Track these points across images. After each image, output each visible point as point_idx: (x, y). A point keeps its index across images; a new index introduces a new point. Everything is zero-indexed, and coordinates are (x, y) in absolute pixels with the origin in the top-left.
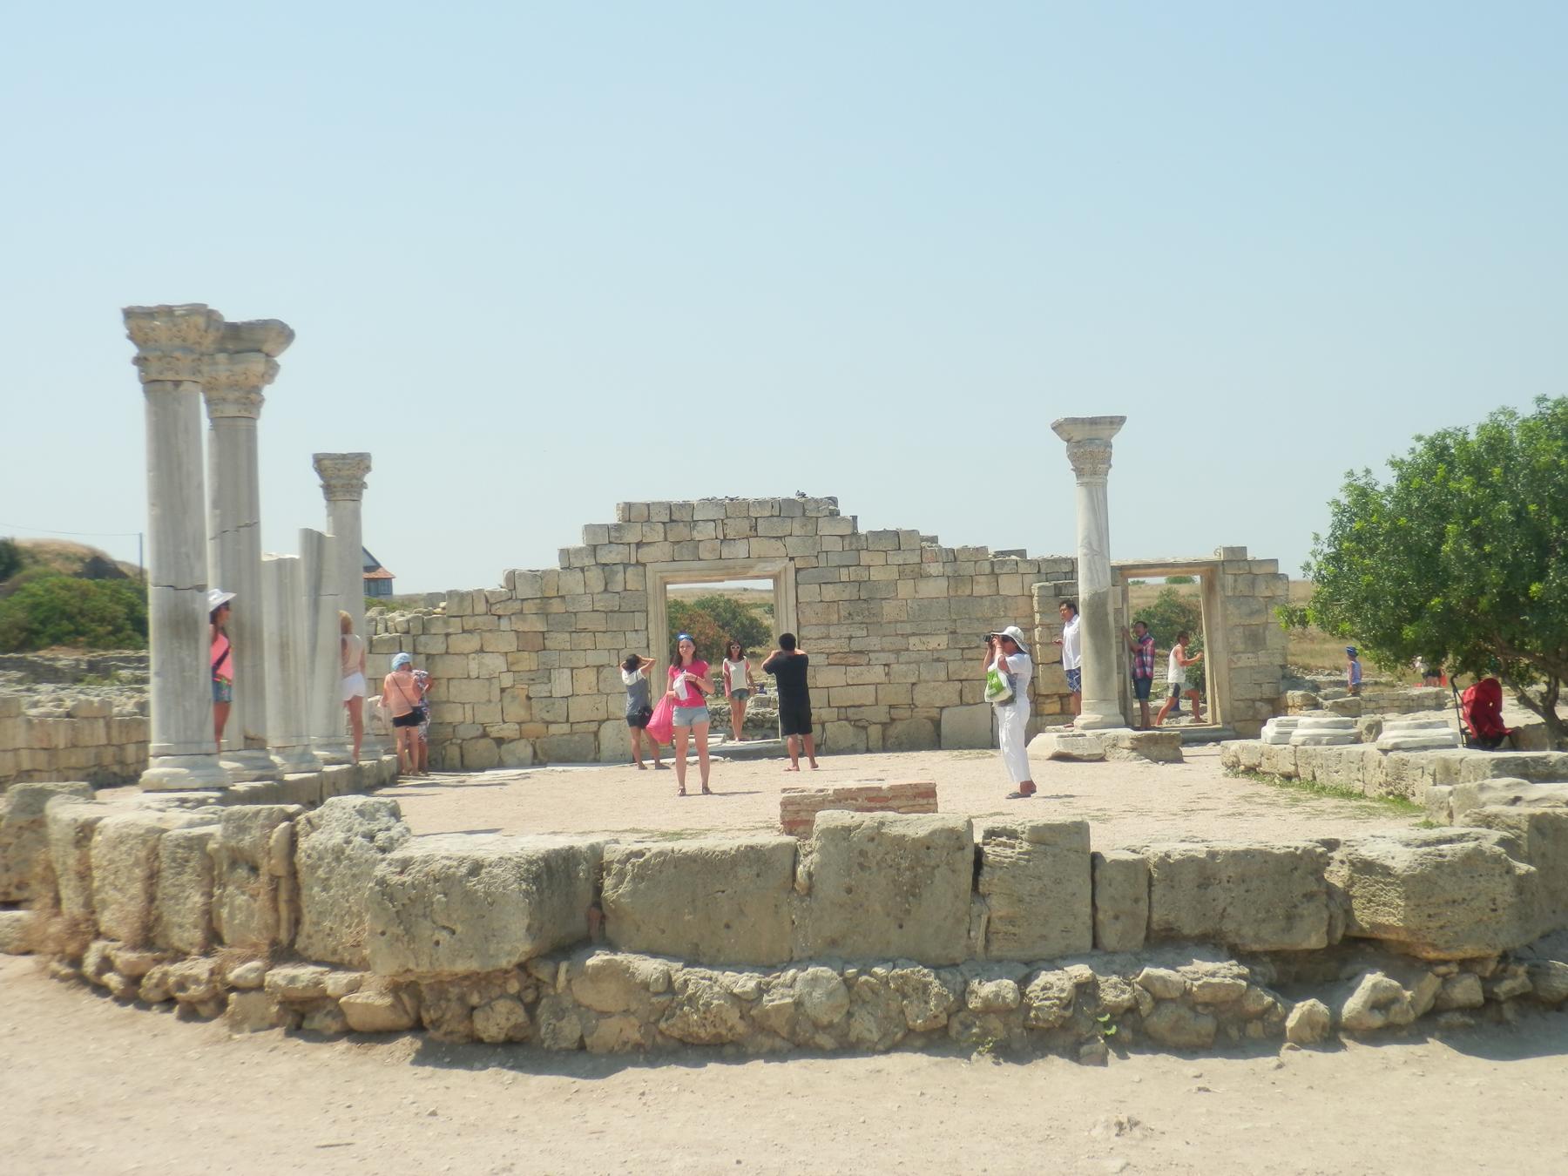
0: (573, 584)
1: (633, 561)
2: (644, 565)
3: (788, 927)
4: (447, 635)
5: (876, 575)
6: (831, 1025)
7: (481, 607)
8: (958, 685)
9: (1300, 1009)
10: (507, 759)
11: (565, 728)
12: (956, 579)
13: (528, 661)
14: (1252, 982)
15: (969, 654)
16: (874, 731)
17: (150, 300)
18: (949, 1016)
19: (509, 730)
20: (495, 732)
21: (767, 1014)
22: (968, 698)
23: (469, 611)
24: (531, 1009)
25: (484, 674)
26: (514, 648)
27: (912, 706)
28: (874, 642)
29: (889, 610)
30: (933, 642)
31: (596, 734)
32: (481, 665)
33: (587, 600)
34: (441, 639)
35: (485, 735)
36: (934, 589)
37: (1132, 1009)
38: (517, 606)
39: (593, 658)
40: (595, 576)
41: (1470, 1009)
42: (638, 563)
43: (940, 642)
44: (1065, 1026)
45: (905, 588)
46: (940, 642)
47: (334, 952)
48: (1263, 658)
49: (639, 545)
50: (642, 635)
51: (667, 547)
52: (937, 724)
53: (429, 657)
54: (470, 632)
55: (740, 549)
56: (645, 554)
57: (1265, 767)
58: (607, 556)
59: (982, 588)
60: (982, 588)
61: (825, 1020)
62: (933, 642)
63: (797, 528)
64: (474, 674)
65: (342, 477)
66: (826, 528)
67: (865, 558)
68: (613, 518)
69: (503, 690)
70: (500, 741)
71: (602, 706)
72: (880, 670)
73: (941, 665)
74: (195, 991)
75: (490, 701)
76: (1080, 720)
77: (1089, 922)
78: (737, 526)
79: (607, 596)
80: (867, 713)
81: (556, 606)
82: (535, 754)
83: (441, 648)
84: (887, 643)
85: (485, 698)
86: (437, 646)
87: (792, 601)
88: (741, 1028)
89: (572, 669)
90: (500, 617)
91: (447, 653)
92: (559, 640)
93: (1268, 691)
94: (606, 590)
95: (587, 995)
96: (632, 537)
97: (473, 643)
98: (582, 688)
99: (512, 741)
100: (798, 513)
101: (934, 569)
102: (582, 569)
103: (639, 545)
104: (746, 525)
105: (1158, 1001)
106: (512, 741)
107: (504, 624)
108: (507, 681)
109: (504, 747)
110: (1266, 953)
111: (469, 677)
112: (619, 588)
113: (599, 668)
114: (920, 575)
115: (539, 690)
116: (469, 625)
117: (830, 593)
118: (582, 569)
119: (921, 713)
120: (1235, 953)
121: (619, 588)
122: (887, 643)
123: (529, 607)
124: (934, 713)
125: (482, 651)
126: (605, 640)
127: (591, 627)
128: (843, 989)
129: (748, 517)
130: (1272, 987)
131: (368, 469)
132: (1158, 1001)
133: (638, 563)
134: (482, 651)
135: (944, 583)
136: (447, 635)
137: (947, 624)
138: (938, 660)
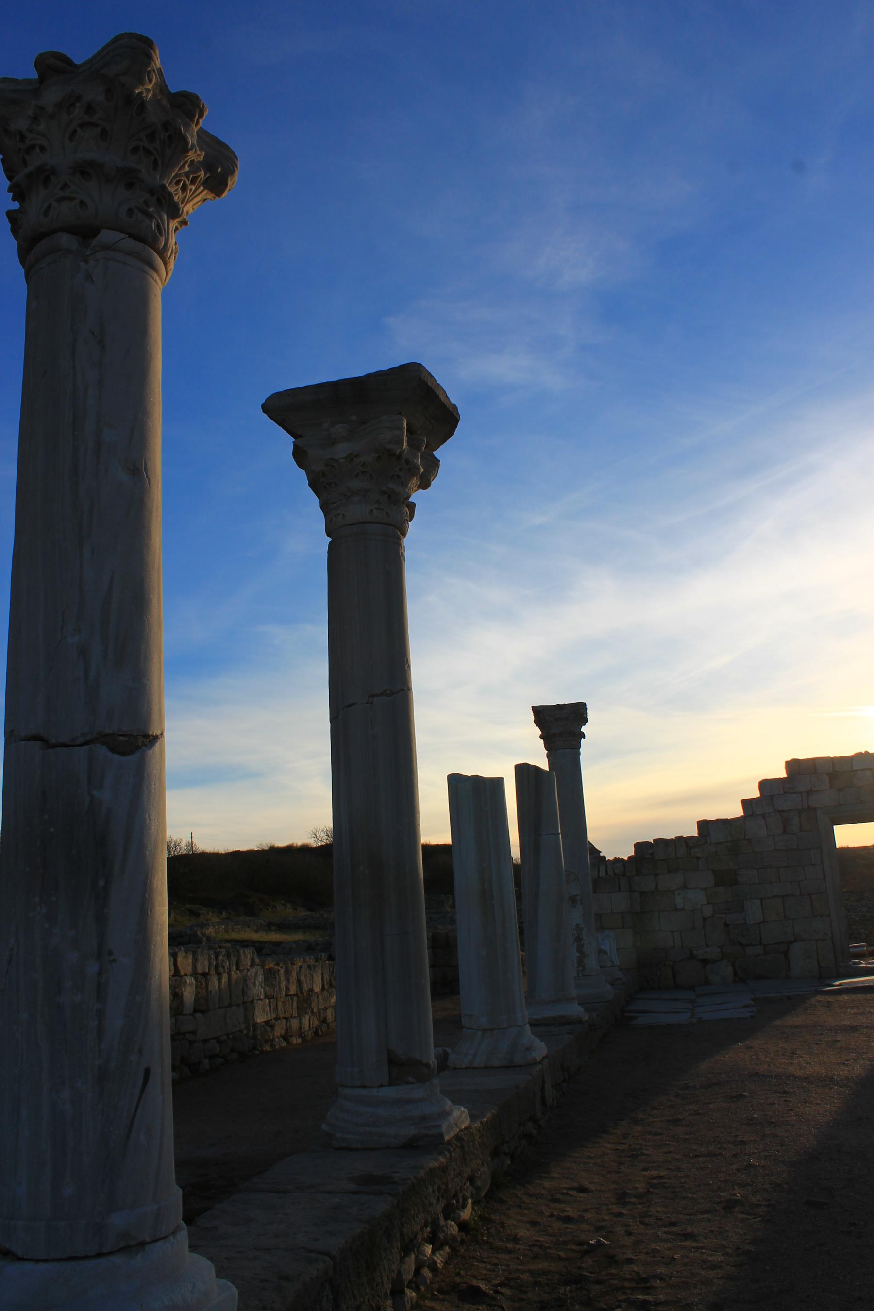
2: (815, 809)
4: (656, 875)
35: (692, 957)
53: (642, 894)
68: (781, 773)
69: (705, 919)
70: (705, 962)
82: (735, 973)
89: (762, 899)
94: (785, 832)
102: (764, 816)
108: (708, 911)
111: (676, 909)
118: (764, 816)
125: (685, 887)
131: (585, 721)
134: (685, 887)
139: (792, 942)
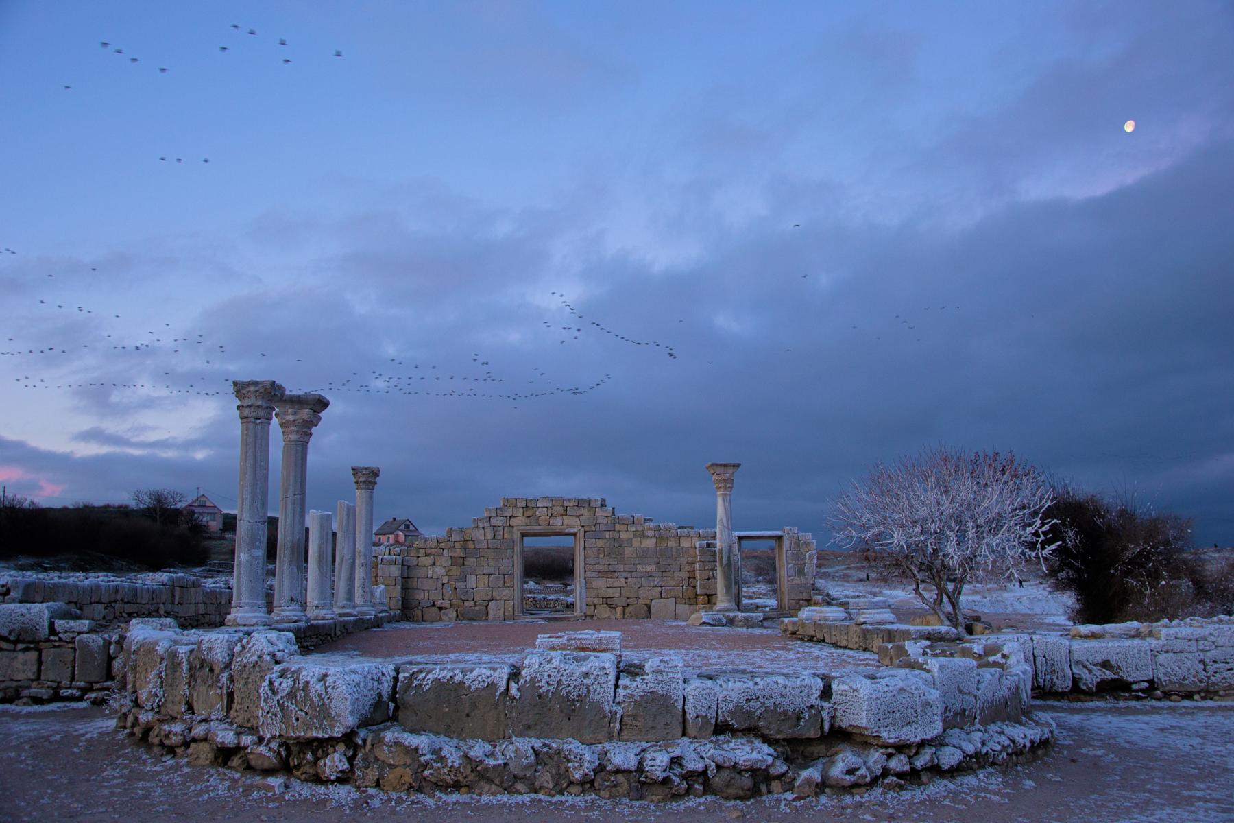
0: (479, 534)
3: (503, 716)
5: (622, 535)
6: (524, 777)
7: (435, 544)
9: (805, 774)
10: (444, 618)
11: (472, 603)
12: (660, 538)
13: (456, 571)
14: (775, 758)
16: (619, 610)
17: (245, 377)
18: (595, 774)
19: (446, 603)
20: (438, 604)
21: (486, 769)
24: (351, 760)
25: (435, 576)
27: (638, 598)
28: (621, 567)
29: (628, 552)
30: (648, 568)
35: (434, 605)
36: (650, 543)
37: (704, 773)
38: (451, 544)
41: (900, 775)
43: (651, 568)
44: (666, 781)
45: (636, 542)
46: (653, 567)
47: (249, 721)
48: (803, 580)
51: (524, 519)
56: (514, 522)
57: (801, 631)
58: (494, 522)
60: (672, 544)
61: (521, 774)
62: (648, 568)
63: (586, 513)
66: (599, 512)
67: (618, 527)
70: (441, 609)
72: (623, 580)
74: (174, 740)
76: (717, 607)
77: (681, 720)
80: (616, 601)
81: (471, 545)
84: (627, 568)
88: (471, 778)
92: (471, 561)
93: (806, 596)
95: (383, 753)
97: (430, 560)
98: (481, 585)
101: (650, 533)
104: (560, 510)
105: (719, 767)
108: (445, 580)
110: (784, 740)
114: (644, 536)
115: (459, 585)
116: (428, 551)
117: (600, 543)
119: (641, 602)
120: (766, 740)
122: (627, 568)
123: (457, 545)
125: (434, 564)
126: (492, 562)
128: (533, 757)
130: (787, 760)
132: (719, 767)
134: (434, 564)
135: (654, 540)
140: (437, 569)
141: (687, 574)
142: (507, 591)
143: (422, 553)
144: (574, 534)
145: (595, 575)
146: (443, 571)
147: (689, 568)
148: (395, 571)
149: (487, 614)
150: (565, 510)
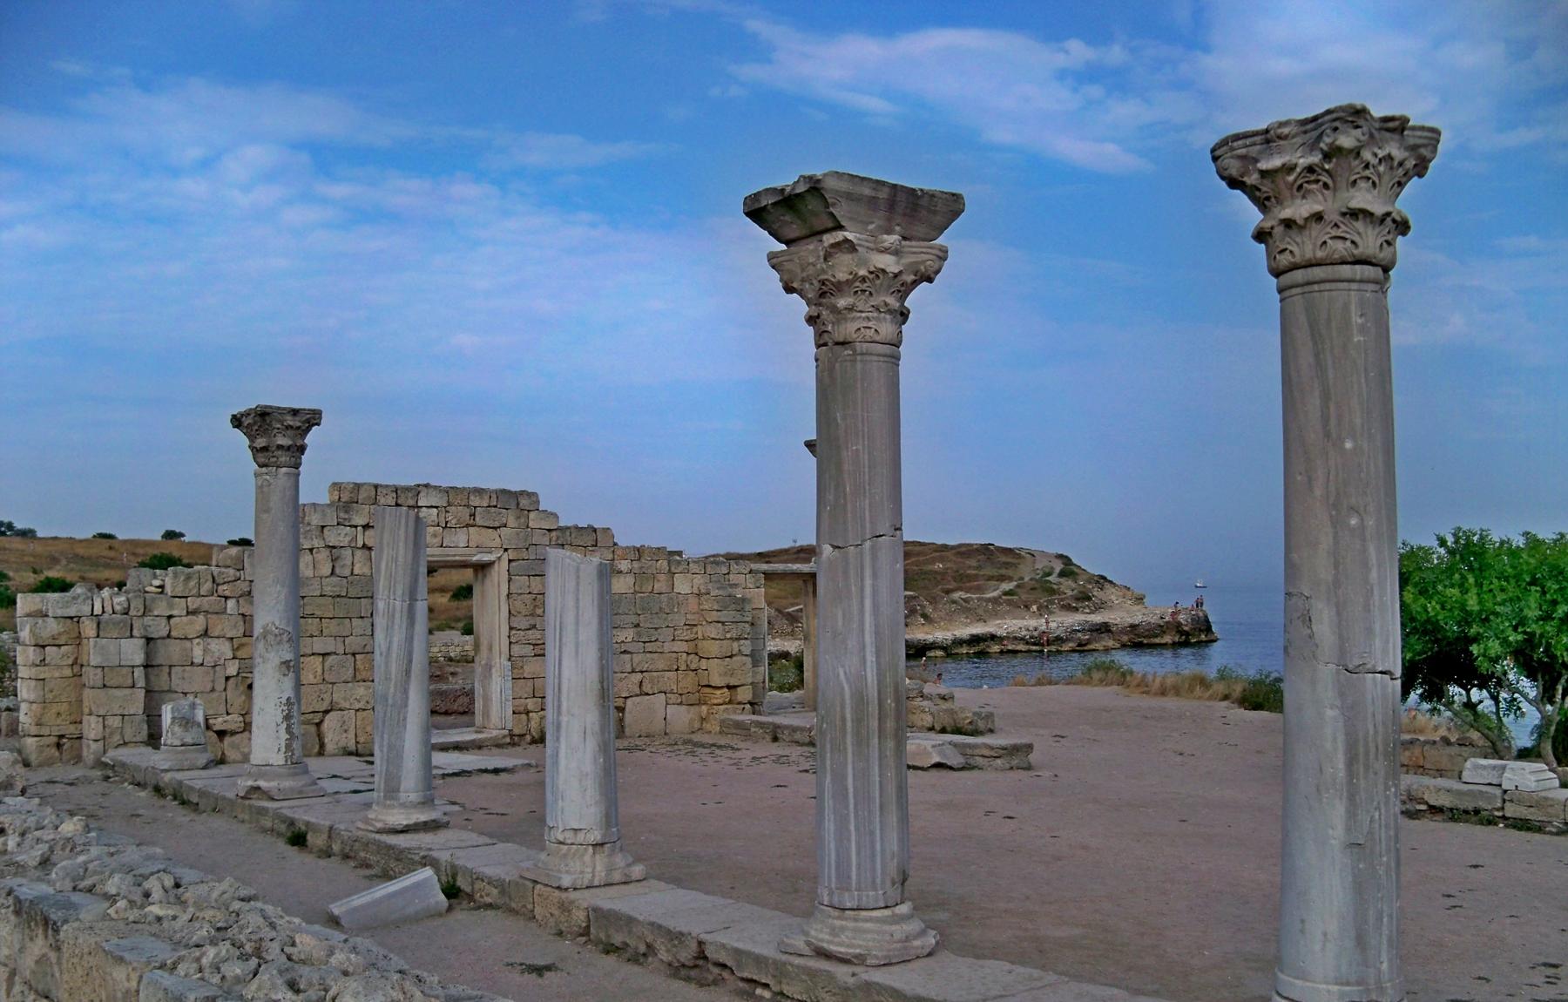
1: (360, 544)
2: (370, 549)
4: (170, 617)
7: (207, 586)
8: (639, 676)
12: (640, 576)
15: (649, 647)
20: (218, 723)
22: (647, 688)
23: (194, 591)
25: (209, 661)
26: (240, 633)
31: (318, 725)
32: (205, 651)
33: (316, 584)
34: (164, 621)
39: (319, 645)
40: (323, 555)
42: (364, 546)
49: (366, 527)
50: (367, 622)
52: (621, 709)
53: (149, 640)
54: (194, 613)
55: (460, 538)
58: (332, 537)
59: (660, 586)
60: (660, 586)
63: (512, 522)
64: (198, 660)
65: (276, 433)
69: (227, 679)
70: (221, 734)
71: (327, 697)
73: (627, 657)
75: (213, 690)
78: (458, 513)
79: (334, 579)
83: (164, 633)
85: (209, 687)
86: (159, 629)
87: (505, 591)
90: (226, 598)
91: (169, 636)
94: (332, 573)
96: (360, 520)
97: (199, 622)
99: (233, 733)
100: (513, 506)
101: (624, 565)
102: (311, 550)
103: (366, 527)
106: (233, 733)
107: (231, 604)
109: (227, 740)
112: (347, 572)
113: (324, 655)
116: (193, 603)
121: (347, 572)
124: (620, 703)
126: (331, 627)
127: (318, 613)
129: (468, 506)
133: (364, 546)
134: (205, 634)
135: (630, 579)
136: (170, 617)
137: (634, 619)
138: (625, 652)
139: (326, 712)
140: (215, 645)
141: (684, 647)
142: (361, 690)
143: (179, 608)
144: (482, 568)
145: (528, 650)
146: (225, 649)
147: (687, 635)
148: (133, 651)
149: (322, 745)
150: (473, 515)
